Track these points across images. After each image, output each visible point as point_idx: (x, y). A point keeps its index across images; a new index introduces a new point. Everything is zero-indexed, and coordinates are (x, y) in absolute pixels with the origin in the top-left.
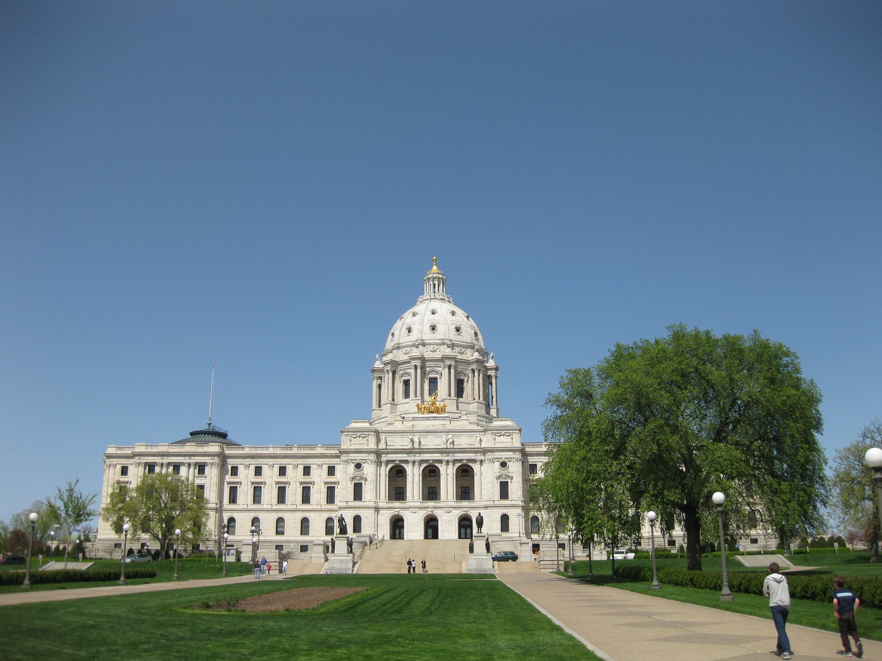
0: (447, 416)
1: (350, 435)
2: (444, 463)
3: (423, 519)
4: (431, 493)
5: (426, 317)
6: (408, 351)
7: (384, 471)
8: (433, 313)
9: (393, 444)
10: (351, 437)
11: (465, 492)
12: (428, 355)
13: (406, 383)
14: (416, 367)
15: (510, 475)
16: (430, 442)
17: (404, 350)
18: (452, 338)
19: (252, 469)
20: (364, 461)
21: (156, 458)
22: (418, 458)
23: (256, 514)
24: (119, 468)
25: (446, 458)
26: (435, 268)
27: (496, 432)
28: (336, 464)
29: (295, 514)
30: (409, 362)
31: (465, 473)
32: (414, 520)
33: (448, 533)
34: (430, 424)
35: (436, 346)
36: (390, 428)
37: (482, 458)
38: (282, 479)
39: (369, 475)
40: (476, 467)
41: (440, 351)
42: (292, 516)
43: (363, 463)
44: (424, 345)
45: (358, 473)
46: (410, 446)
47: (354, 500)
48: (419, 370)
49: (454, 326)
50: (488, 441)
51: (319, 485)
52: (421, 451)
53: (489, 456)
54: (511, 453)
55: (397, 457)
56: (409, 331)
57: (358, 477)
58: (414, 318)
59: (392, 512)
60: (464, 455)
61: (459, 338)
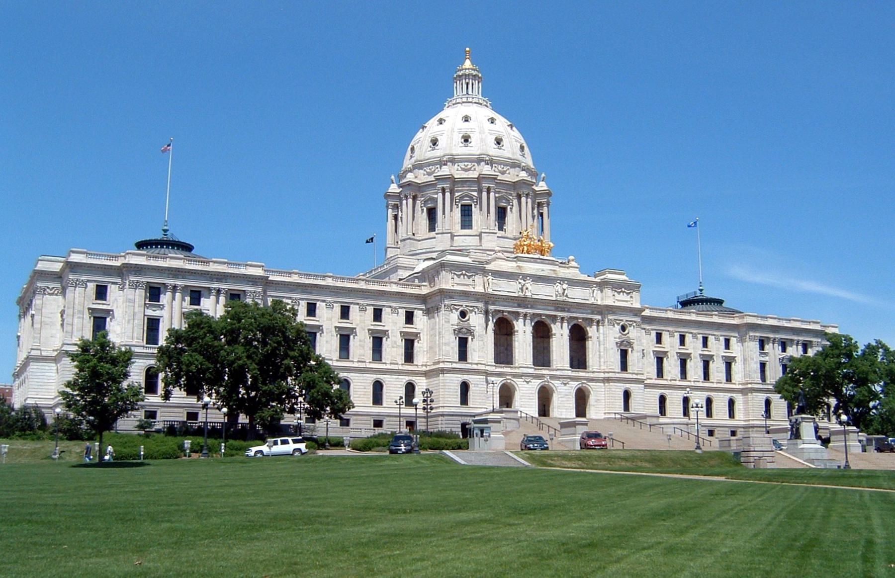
1: (453, 272)
4: (542, 357)
6: (469, 167)
7: (491, 325)
10: (454, 274)
11: (579, 360)
19: (303, 306)
26: (468, 64)
28: (415, 309)
29: (364, 375)
31: (578, 336)
32: (527, 392)
33: (565, 410)
34: (538, 267)
39: (477, 328)
40: (591, 331)
41: (509, 174)
42: (362, 378)
43: (469, 310)
48: (448, 195)
50: (608, 298)
57: (464, 330)
58: (467, 123)
59: (502, 379)
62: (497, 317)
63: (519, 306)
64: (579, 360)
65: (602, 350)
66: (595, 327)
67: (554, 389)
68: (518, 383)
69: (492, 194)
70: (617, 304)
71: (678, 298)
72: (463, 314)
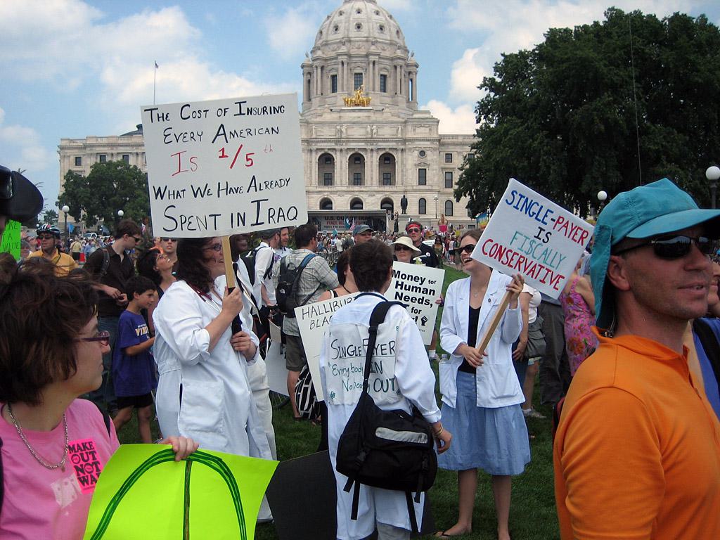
0: (371, 108)
3: (349, 202)
4: (357, 179)
5: (352, 15)
7: (316, 157)
8: (359, 13)
11: (387, 179)
12: (354, 52)
13: (334, 78)
14: (343, 63)
15: (428, 163)
16: (357, 132)
17: (331, 47)
18: (377, 35)
21: (106, 148)
22: (344, 147)
24: (72, 158)
25: (371, 147)
30: (336, 58)
31: (387, 160)
35: (361, 43)
36: (318, 119)
37: (403, 147)
40: (398, 156)
44: (350, 41)
49: (378, 25)
52: (348, 140)
53: (409, 145)
54: (429, 143)
55: (326, 146)
56: (336, 30)
61: (382, 36)
62: (320, 154)
63: (336, 145)
64: (387, 179)
66: (400, 154)
67: (363, 200)
69: (345, 65)
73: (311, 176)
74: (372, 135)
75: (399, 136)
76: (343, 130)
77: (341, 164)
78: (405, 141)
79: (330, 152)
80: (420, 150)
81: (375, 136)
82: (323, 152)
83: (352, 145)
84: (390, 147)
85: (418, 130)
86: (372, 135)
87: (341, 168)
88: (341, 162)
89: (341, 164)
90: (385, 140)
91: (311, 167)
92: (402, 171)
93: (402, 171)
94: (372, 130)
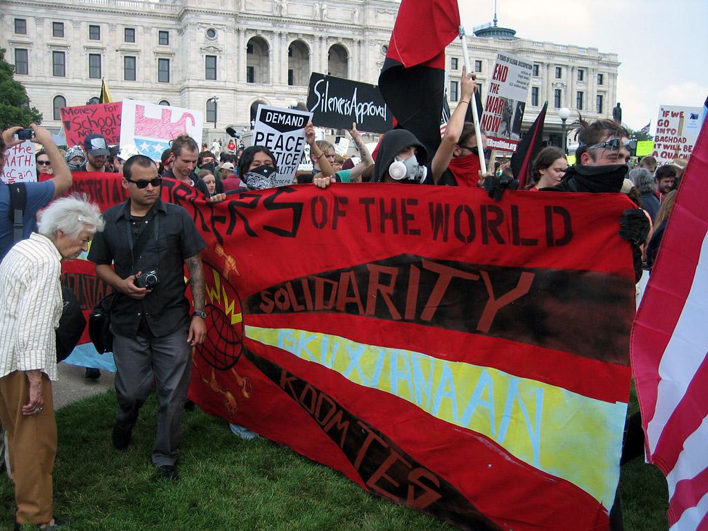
2: (317, 40)
9: (253, 8)
20: (220, 27)
22: (287, 31)
23: (60, 91)
25: (320, 34)
27: (380, 7)
28: (170, 28)
38: (94, 43)
40: (352, 50)
45: (212, 43)
46: (276, 13)
47: (206, 79)
51: (147, 56)
52: (291, 21)
53: (370, 36)
59: (253, 97)
60: (341, 31)
65: (362, 70)
68: (271, 101)
70: (378, 25)
71: (474, 29)
72: (211, 32)
73: (238, 69)
74: (322, 17)
75: (356, 22)
76: (284, 5)
77: (279, 51)
78: (364, 29)
79: (263, 36)
80: (383, 44)
81: (325, 19)
82: (254, 35)
83: (296, 29)
84: (345, 36)
85: (382, 17)
86: (322, 17)
87: (280, 61)
88: (280, 51)
89: (279, 51)
90: (338, 26)
91: (238, 55)
92: (359, 71)
93: (359, 71)
94: (322, 10)
